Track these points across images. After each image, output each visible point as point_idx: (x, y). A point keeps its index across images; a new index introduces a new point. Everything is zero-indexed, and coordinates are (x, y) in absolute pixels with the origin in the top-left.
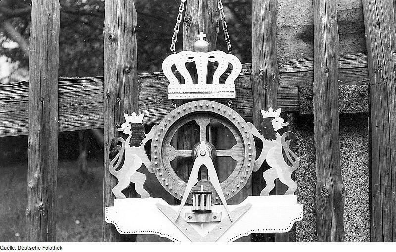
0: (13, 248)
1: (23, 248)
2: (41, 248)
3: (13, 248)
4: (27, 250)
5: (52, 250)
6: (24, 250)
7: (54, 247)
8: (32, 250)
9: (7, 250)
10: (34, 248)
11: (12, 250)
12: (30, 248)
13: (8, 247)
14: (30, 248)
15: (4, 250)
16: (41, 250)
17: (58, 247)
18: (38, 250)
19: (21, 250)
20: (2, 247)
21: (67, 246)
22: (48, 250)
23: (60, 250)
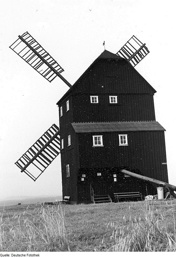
0: (8, 255)
1: (14, 255)
2: (26, 255)
3: (8, 255)
4: (17, 257)
5: (33, 257)
6: (15, 257)
7: (34, 255)
8: (20, 257)
9: (4, 257)
10: (21, 256)
11: (8, 257)
12: (19, 256)
13: (5, 255)
14: (19, 256)
15: (2, 257)
16: (26, 257)
17: (37, 255)
18: (24, 257)
19: (13, 257)
20: (1, 255)
21: (42, 254)
22: (30, 257)
23: (38, 257)
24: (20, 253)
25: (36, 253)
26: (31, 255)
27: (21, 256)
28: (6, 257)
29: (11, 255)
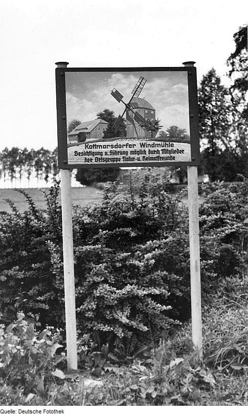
0: (13, 412)
1: (23, 412)
2: (42, 412)
3: (13, 412)
4: (28, 414)
5: (54, 414)
6: (25, 414)
7: (55, 411)
9: (7, 414)
10: (34, 412)
11: (12, 414)
12: (31, 412)
13: (9, 411)
14: (31, 412)
15: (4, 414)
16: (42, 414)
17: (60, 411)
18: (39, 414)
19: (22, 414)
20: (2, 411)
22: (49, 414)
24: (33, 408)
25: (59, 408)
26: (49, 412)
27: (34, 412)
28: (10, 414)
29: (17, 412)
